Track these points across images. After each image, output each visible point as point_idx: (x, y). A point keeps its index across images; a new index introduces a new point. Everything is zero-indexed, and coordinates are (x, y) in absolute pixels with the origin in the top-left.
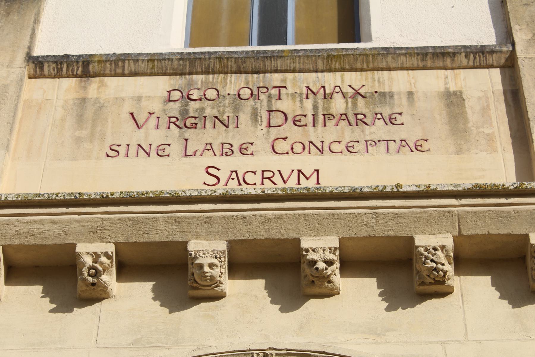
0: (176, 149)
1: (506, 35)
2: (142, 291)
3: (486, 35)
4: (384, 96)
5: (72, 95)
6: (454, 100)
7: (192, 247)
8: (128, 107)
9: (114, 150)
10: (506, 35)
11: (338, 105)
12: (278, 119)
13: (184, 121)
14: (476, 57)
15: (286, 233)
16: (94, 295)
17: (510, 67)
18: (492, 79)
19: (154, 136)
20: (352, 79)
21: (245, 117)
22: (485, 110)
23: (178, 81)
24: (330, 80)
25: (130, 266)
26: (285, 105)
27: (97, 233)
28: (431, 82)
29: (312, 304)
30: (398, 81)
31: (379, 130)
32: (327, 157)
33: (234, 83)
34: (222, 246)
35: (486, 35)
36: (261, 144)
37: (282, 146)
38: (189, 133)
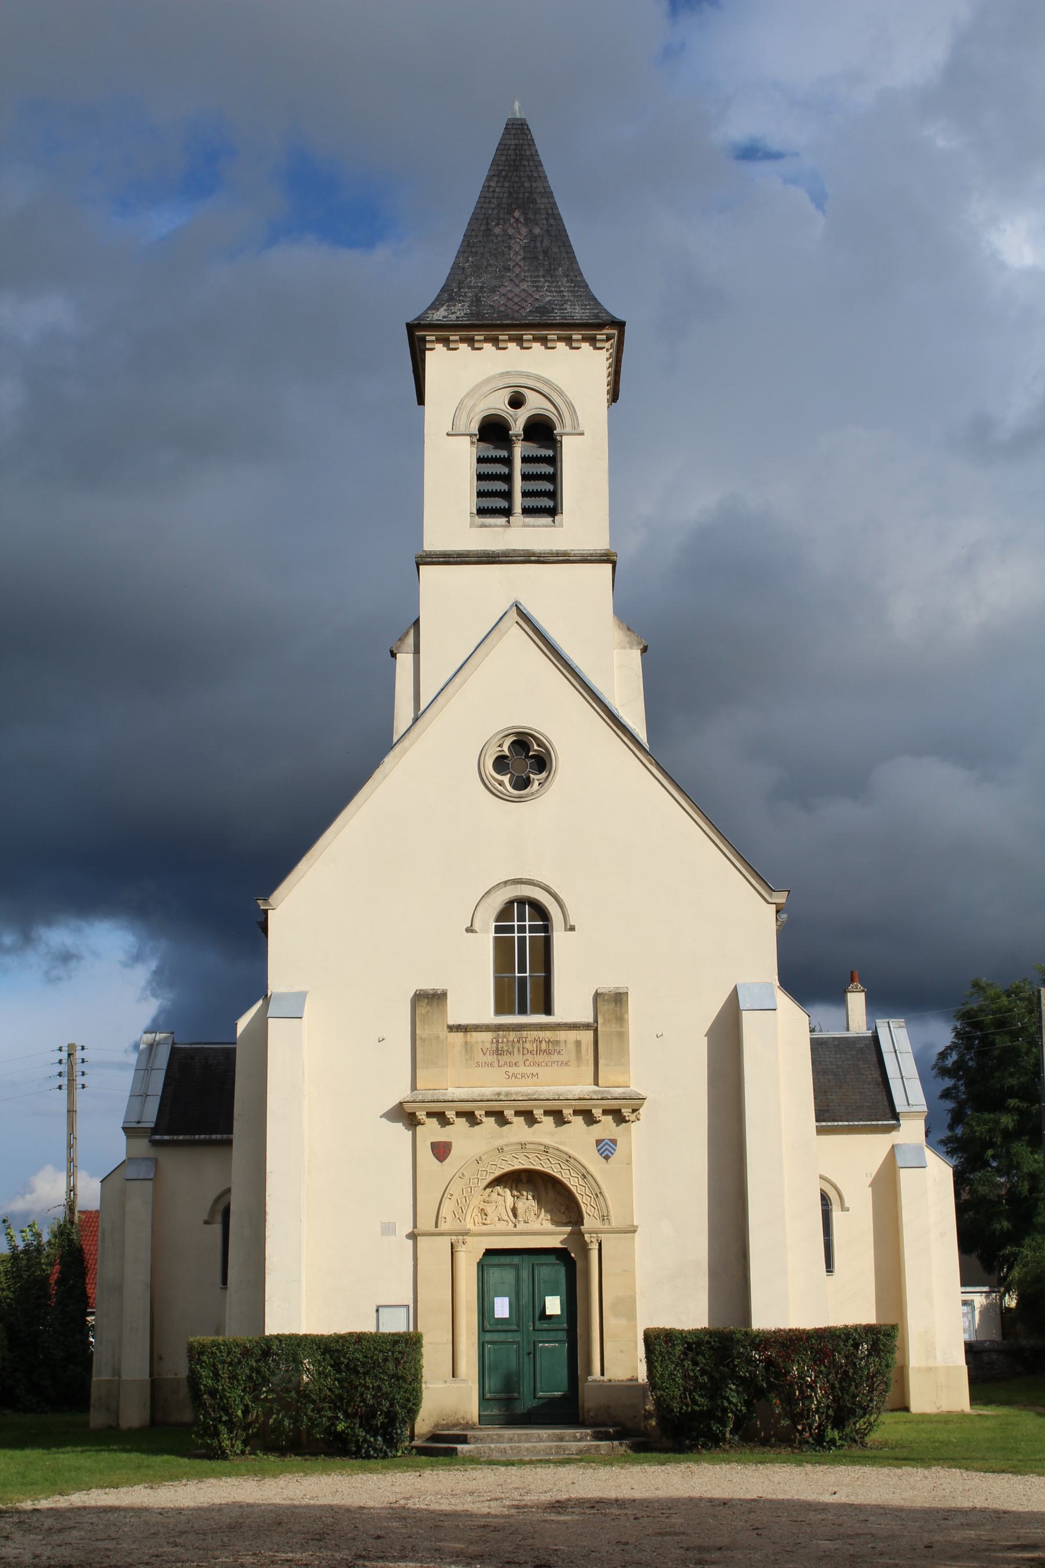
0: (496, 1064)
1: (596, 1021)
2: (492, 1120)
3: (591, 1020)
4: (558, 1042)
5: (462, 1040)
6: (578, 1043)
7: (505, 1113)
8: (480, 1046)
9: (478, 1065)
10: (596, 1021)
11: (544, 1046)
12: (526, 1052)
13: (498, 1052)
14: (586, 1026)
15: (529, 1109)
16: (481, 1122)
17: (596, 1031)
18: (590, 1034)
19: (490, 1058)
20: (548, 1035)
21: (516, 1051)
22: (587, 1049)
23: (494, 1034)
24: (542, 1034)
25: (488, 1114)
26: (527, 1045)
27: (480, 1108)
28: (572, 1035)
29: (536, 1125)
30: (562, 1035)
31: (555, 1057)
32: (541, 1068)
33: (512, 1036)
34: (513, 1112)
35: (591, 1020)
36: (521, 1063)
37: (527, 1063)
38: (500, 1057)
